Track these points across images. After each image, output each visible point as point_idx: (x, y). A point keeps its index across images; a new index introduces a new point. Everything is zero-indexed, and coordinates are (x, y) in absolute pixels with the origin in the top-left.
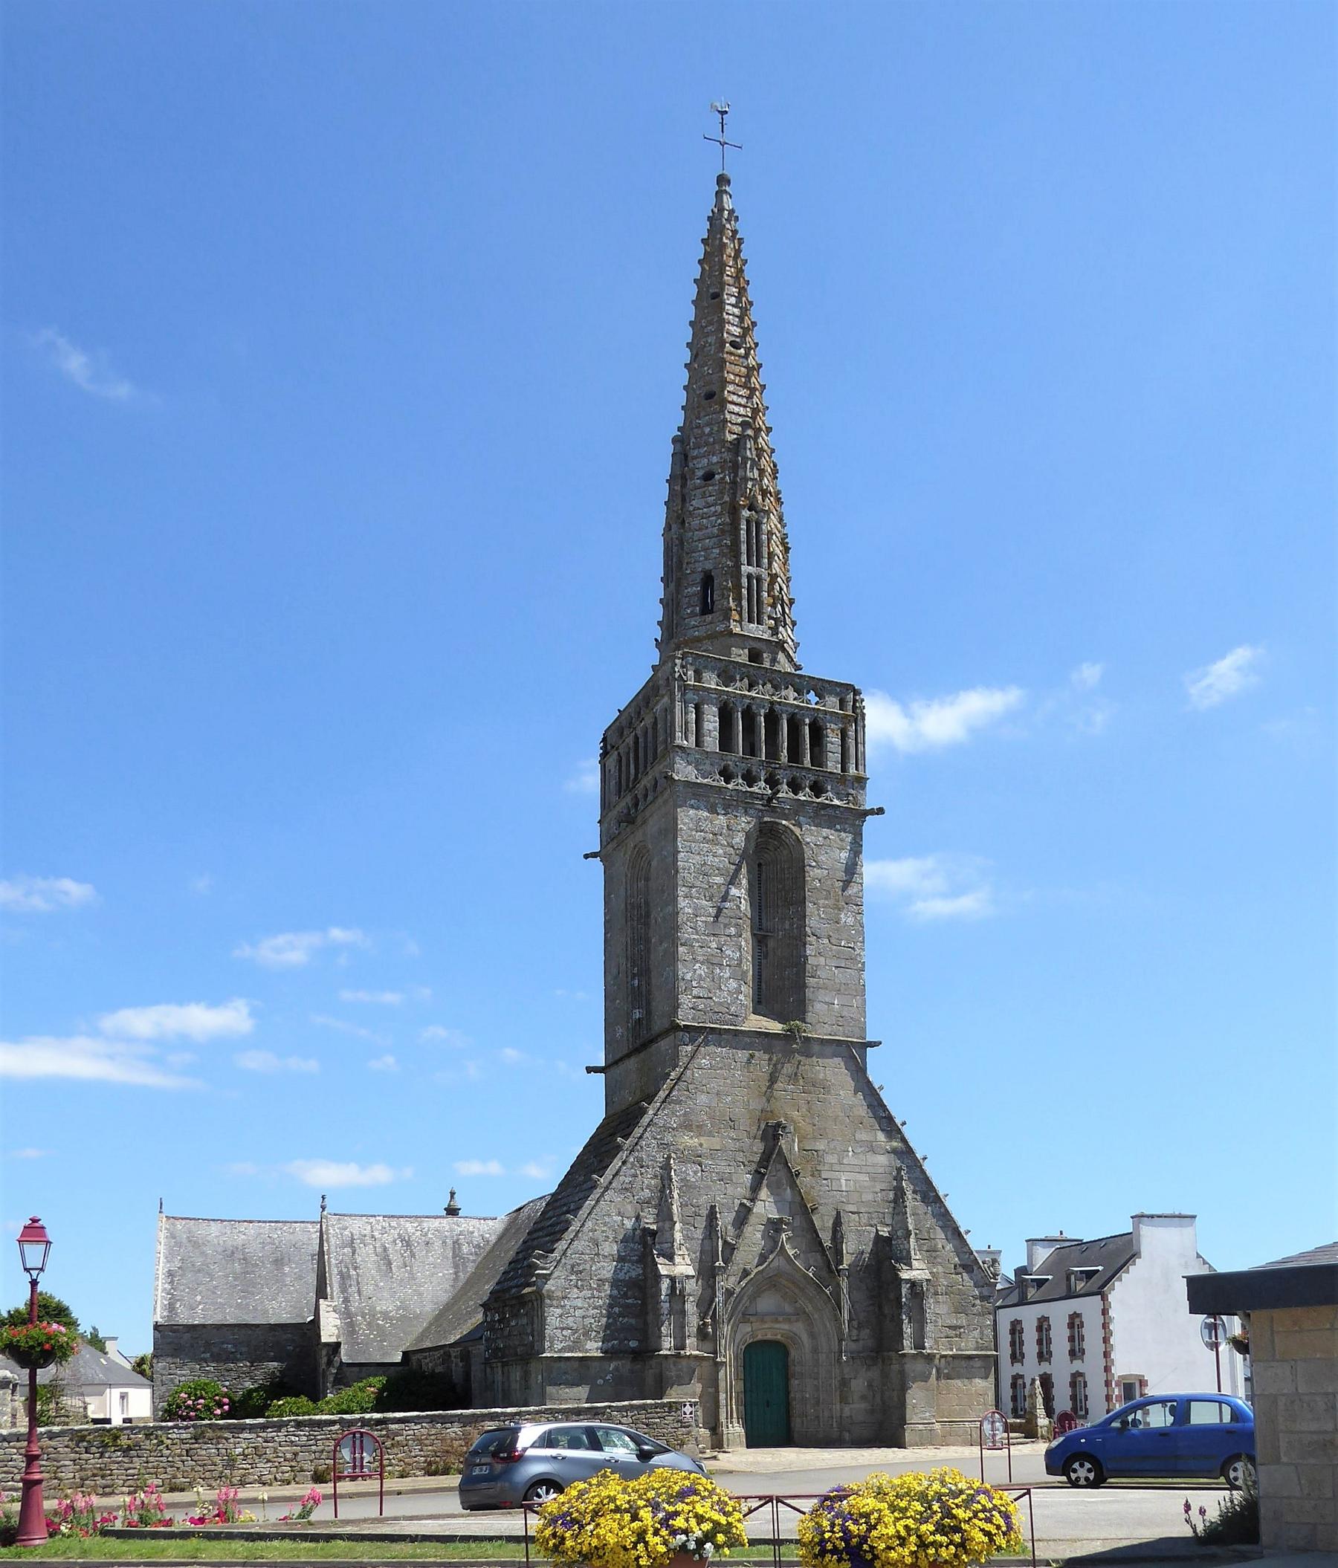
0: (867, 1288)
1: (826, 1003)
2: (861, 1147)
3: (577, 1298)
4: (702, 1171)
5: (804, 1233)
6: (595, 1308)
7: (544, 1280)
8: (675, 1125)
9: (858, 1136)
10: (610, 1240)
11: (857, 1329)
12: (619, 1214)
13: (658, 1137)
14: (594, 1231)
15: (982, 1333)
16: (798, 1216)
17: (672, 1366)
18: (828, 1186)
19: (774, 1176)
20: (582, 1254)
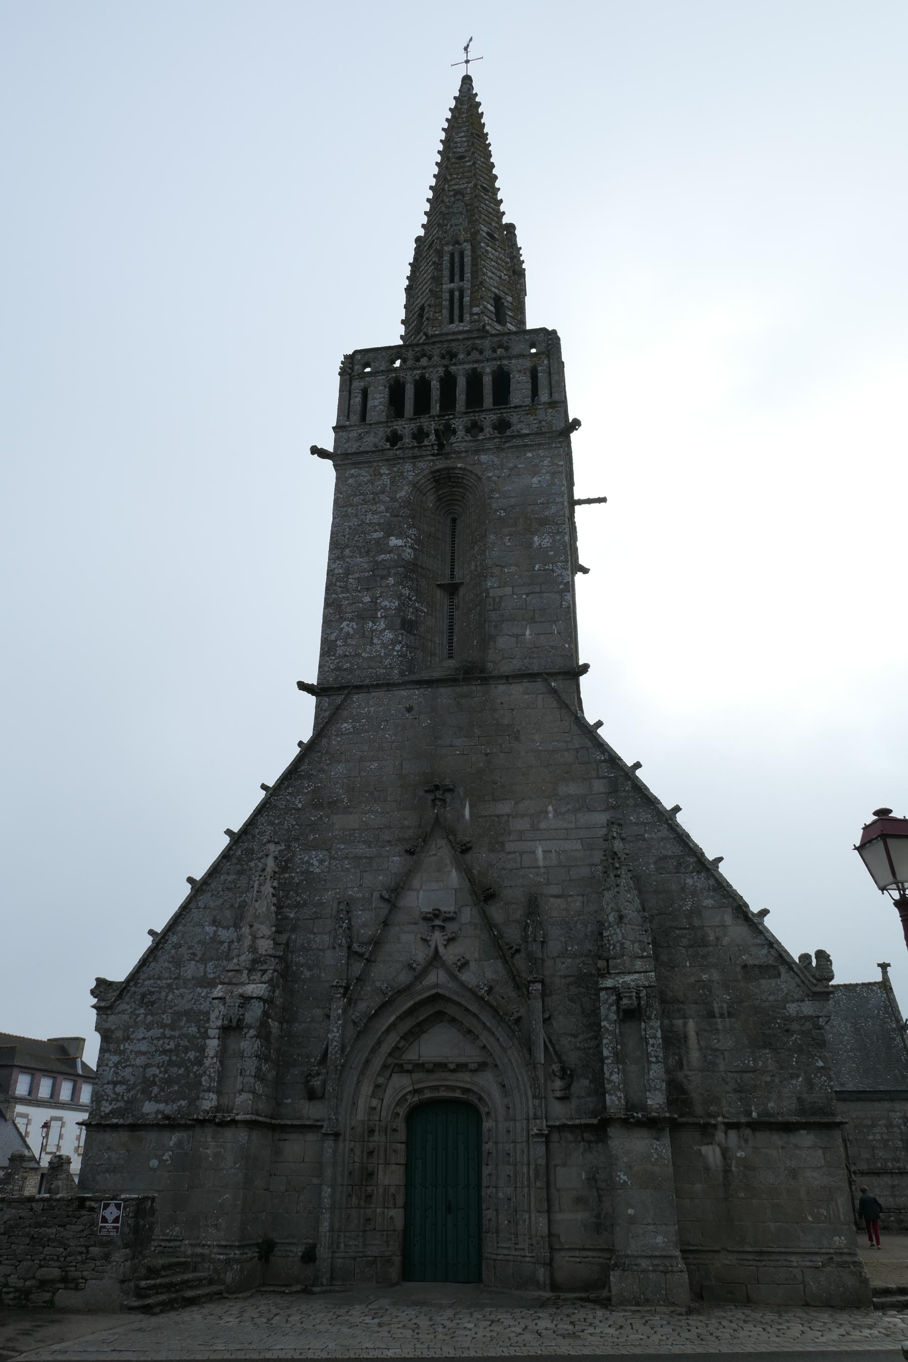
1: (513, 636)
3: (144, 1038)
4: (332, 858)
6: (165, 1052)
7: (104, 1016)
8: (300, 806)
9: (563, 789)
10: (197, 958)
11: (562, 1078)
12: (214, 922)
13: (277, 821)
14: (177, 946)
15: (810, 1084)
16: (468, 909)
17: (209, 1139)
19: (434, 855)
20: (159, 978)
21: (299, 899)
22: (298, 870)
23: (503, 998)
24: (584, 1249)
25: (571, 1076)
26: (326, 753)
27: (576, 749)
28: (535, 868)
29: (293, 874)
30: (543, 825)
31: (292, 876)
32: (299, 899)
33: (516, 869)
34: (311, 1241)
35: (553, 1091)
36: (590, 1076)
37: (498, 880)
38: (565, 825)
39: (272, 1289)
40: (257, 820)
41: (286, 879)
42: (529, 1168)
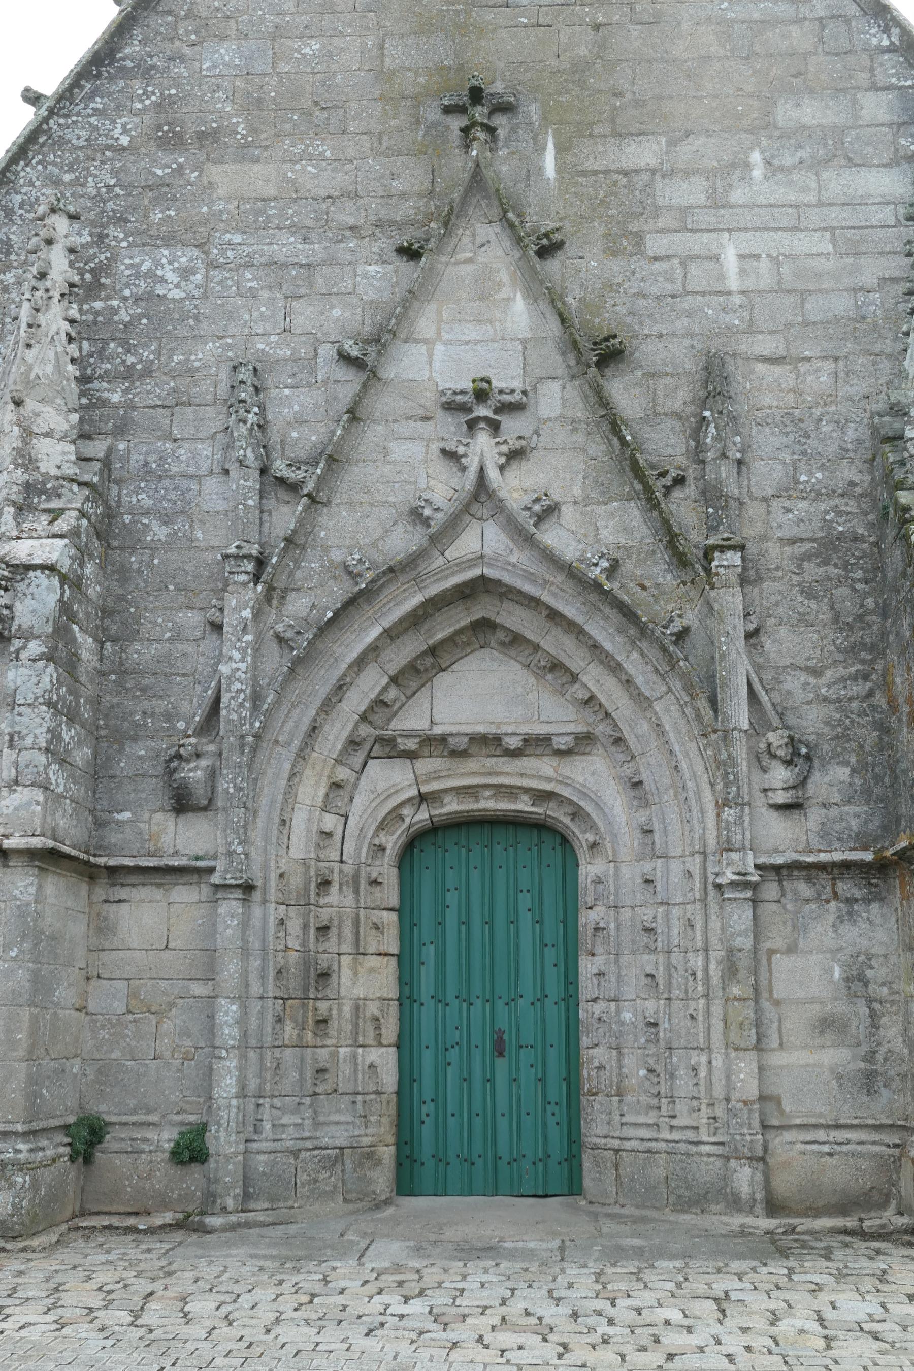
0: (836, 619)
2: (800, 147)
4: (212, 265)
5: (580, 438)
8: (125, 141)
11: (788, 763)
13: (67, 177)
16: (556, 386)
18: (671, 280)
19: (469, 261)
21: (131, 359)
22: (127, 293)
23: (643, 587)
24: (838, 1127)
25: (808, 758)
26: (186, 17)
27: (820, 19)
28: (719, 293)
29: (115, 303)
30: (737, 196)
31: (112, 308)
32: (131, 359)
33: (673, 297)
34: (192, 1118)
35: (765, 790)
36: (853, 759)
37: (628, 320)
38: (792, 197)
39: (106, 1223)
40: (16, 173)
41: (97, 313)
42: (707, 960)
